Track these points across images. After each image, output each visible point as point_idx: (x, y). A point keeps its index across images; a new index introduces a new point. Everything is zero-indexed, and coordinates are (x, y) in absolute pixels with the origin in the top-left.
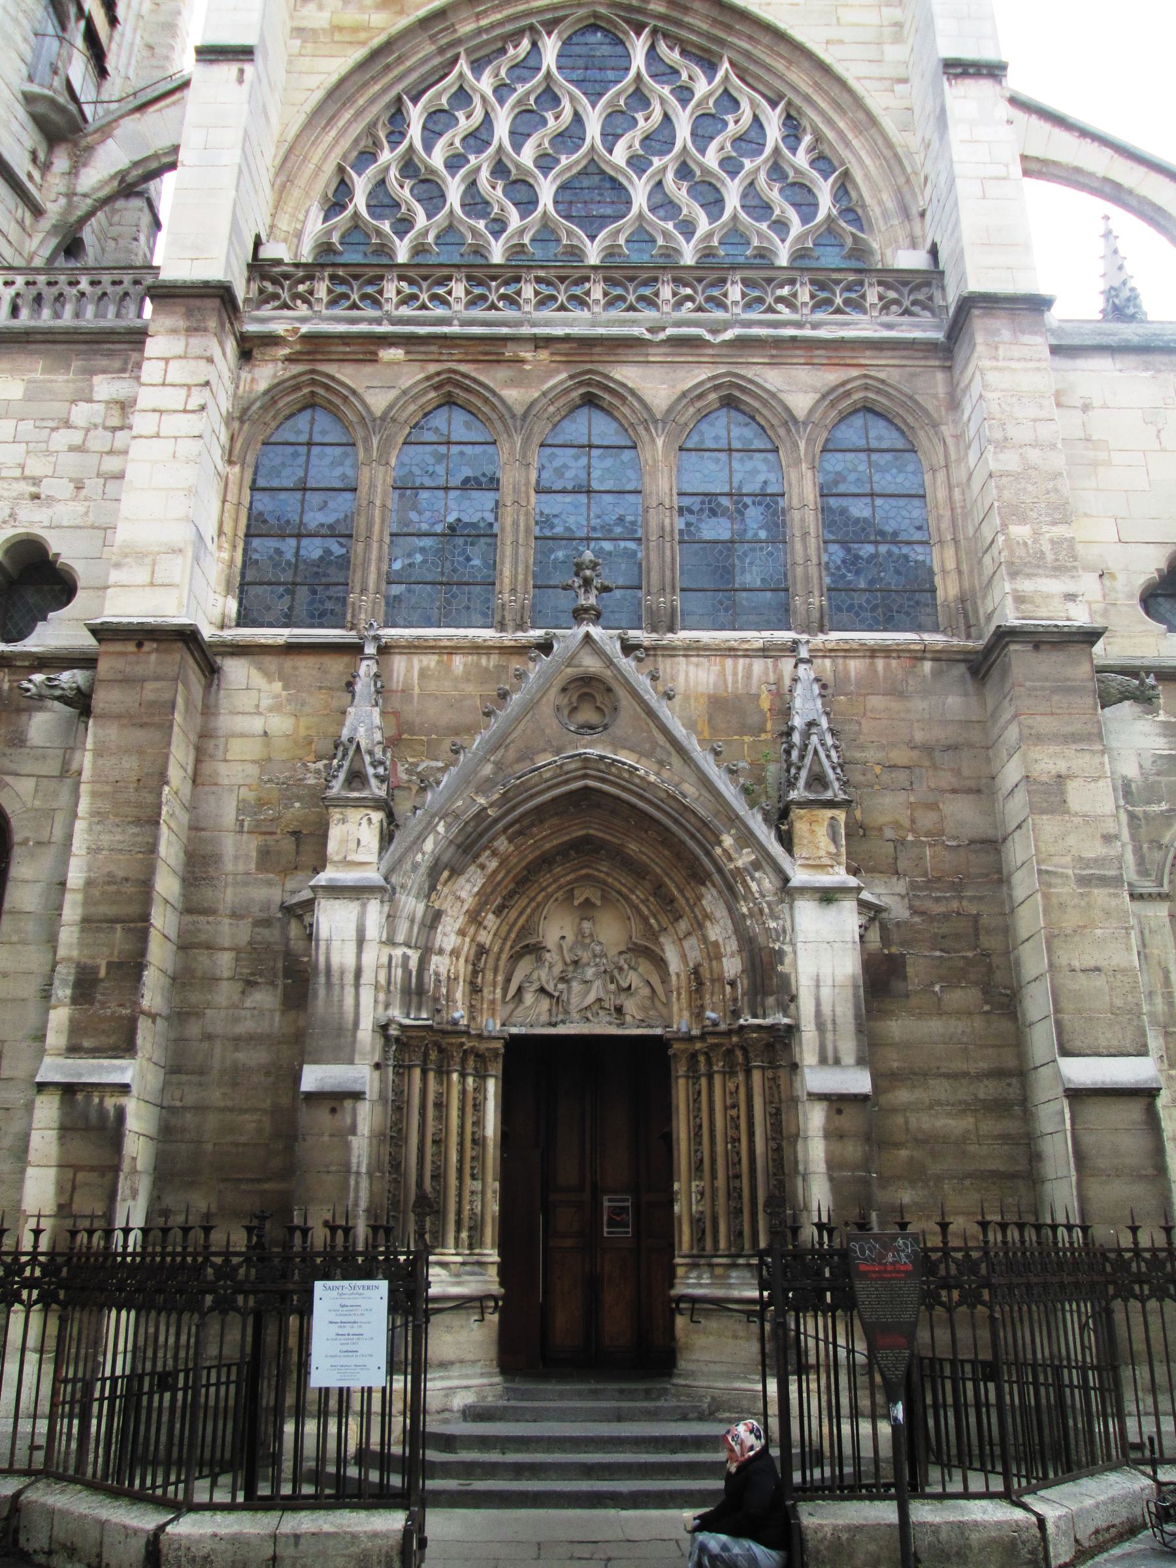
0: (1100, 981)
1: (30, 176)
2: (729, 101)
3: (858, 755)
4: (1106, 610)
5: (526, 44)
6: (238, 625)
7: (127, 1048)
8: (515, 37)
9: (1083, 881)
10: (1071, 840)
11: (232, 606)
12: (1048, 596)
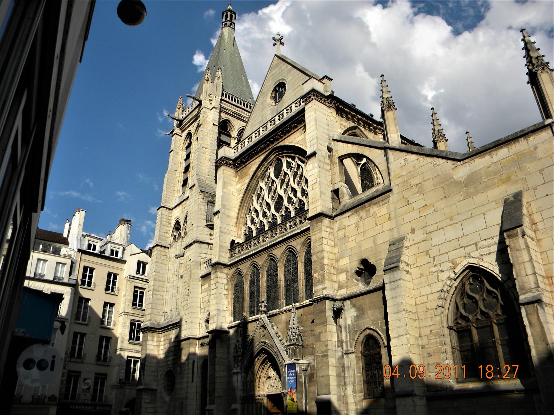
0: (324, 379)
1: (210, 239)
2: (299, 166)
3: (307, 329)
4: (347, 283)
5: (269, 171)
6: (234, 322)
7: (213, 403)
8: (266, 171)
9: (322, 356)
10: (321, 347)
11: (232, 318)
12: (320, 289)
